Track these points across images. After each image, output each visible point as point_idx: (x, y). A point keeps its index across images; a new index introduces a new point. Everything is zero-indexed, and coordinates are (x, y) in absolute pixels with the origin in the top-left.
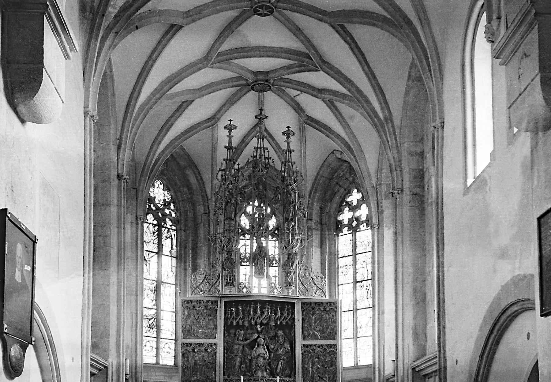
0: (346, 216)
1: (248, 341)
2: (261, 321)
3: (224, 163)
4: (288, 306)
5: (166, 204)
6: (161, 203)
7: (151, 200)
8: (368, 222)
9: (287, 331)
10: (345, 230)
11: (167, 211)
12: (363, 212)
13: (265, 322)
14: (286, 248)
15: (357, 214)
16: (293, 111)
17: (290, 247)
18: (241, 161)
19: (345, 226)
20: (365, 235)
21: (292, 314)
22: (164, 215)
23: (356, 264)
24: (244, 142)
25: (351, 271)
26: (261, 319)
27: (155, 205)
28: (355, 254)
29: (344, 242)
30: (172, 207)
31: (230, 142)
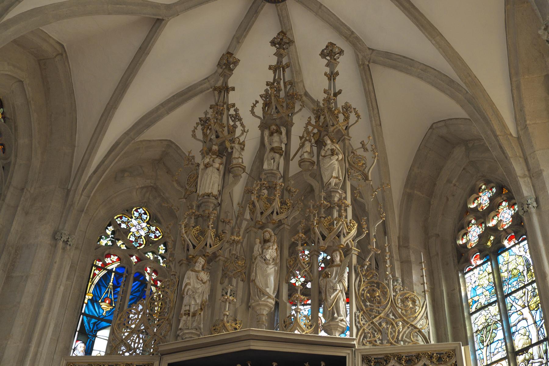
6: (143, 241)
7: (120, 233)
8: (519, 229)
10: (475, 261)
14: (324, 238)
17: (333, 235)
20: (515, 256)
23: (507, 317)
25: (500, 335)
27: (128, 243)
29: (477, 281)
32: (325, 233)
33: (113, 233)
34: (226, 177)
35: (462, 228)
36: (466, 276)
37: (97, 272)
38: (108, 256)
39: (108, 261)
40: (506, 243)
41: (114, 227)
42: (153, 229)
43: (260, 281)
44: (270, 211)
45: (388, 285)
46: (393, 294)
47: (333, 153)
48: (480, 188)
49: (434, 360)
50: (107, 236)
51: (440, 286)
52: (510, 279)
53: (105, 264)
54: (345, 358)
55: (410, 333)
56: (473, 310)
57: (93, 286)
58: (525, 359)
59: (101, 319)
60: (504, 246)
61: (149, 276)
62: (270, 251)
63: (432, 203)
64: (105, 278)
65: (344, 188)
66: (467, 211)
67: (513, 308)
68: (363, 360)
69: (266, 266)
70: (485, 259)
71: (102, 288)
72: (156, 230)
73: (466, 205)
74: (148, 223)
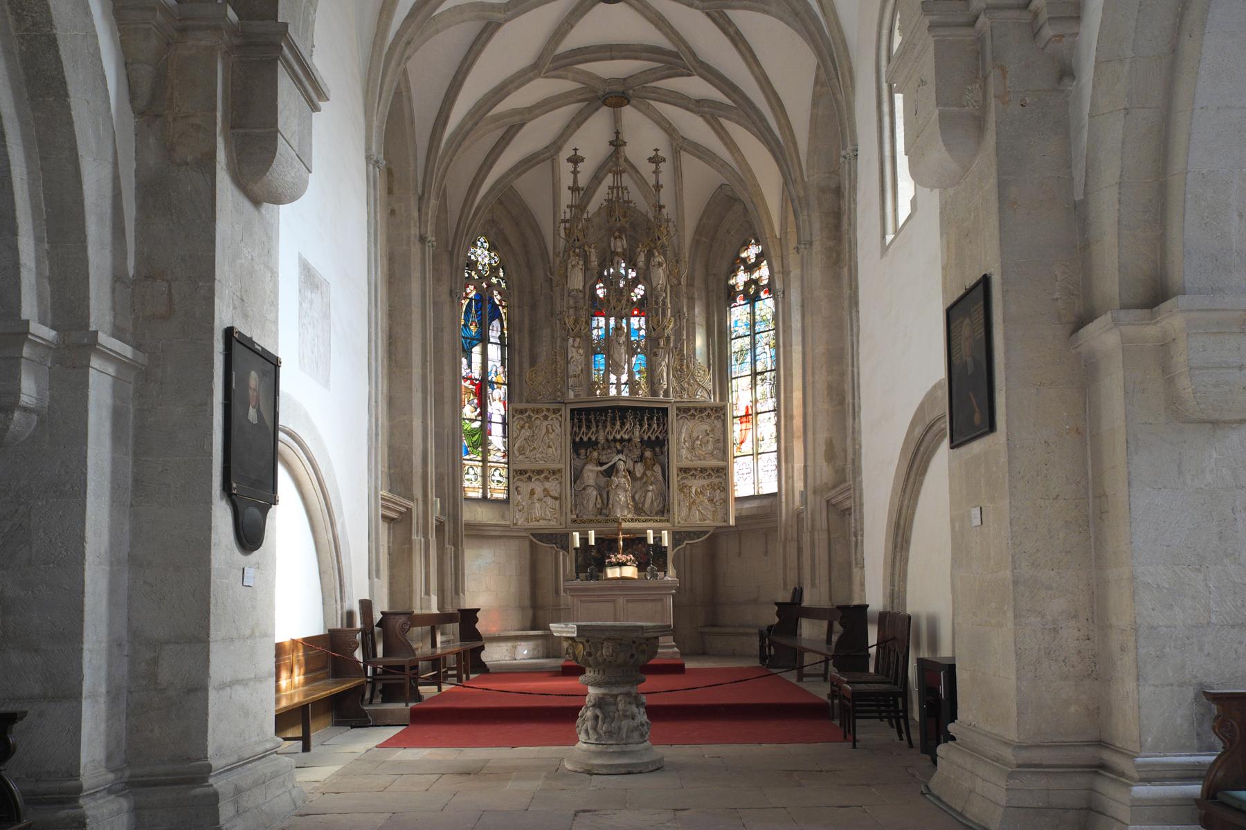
0: (741, 279)
1: (605, 467)
3: (568, 210)
5: (494, 270)
7: (472, 265)
8: (770, 288)
9: (657, 449)
10: (740, 301)
11: (494, 280)
12: (763, 273)
13: (626, 437)
15: (756, 275)
16: (662, 132)
18: (593, 207)
19: (741, 292)
20: (766, 306)
22: (490, 285)
24: (596, 179)
25: (748, 359)
27: (478, 272)
28: (753, 334)
29: (739, 314)
31: (575, 181)
40: (762, 295)
43: (616, 356)
47: (660, 264)
59: (472, 339)
61: (497, 298)
64: (469, 305)
65: (665, 291)
66: (738, 257)
73: (738, 253)
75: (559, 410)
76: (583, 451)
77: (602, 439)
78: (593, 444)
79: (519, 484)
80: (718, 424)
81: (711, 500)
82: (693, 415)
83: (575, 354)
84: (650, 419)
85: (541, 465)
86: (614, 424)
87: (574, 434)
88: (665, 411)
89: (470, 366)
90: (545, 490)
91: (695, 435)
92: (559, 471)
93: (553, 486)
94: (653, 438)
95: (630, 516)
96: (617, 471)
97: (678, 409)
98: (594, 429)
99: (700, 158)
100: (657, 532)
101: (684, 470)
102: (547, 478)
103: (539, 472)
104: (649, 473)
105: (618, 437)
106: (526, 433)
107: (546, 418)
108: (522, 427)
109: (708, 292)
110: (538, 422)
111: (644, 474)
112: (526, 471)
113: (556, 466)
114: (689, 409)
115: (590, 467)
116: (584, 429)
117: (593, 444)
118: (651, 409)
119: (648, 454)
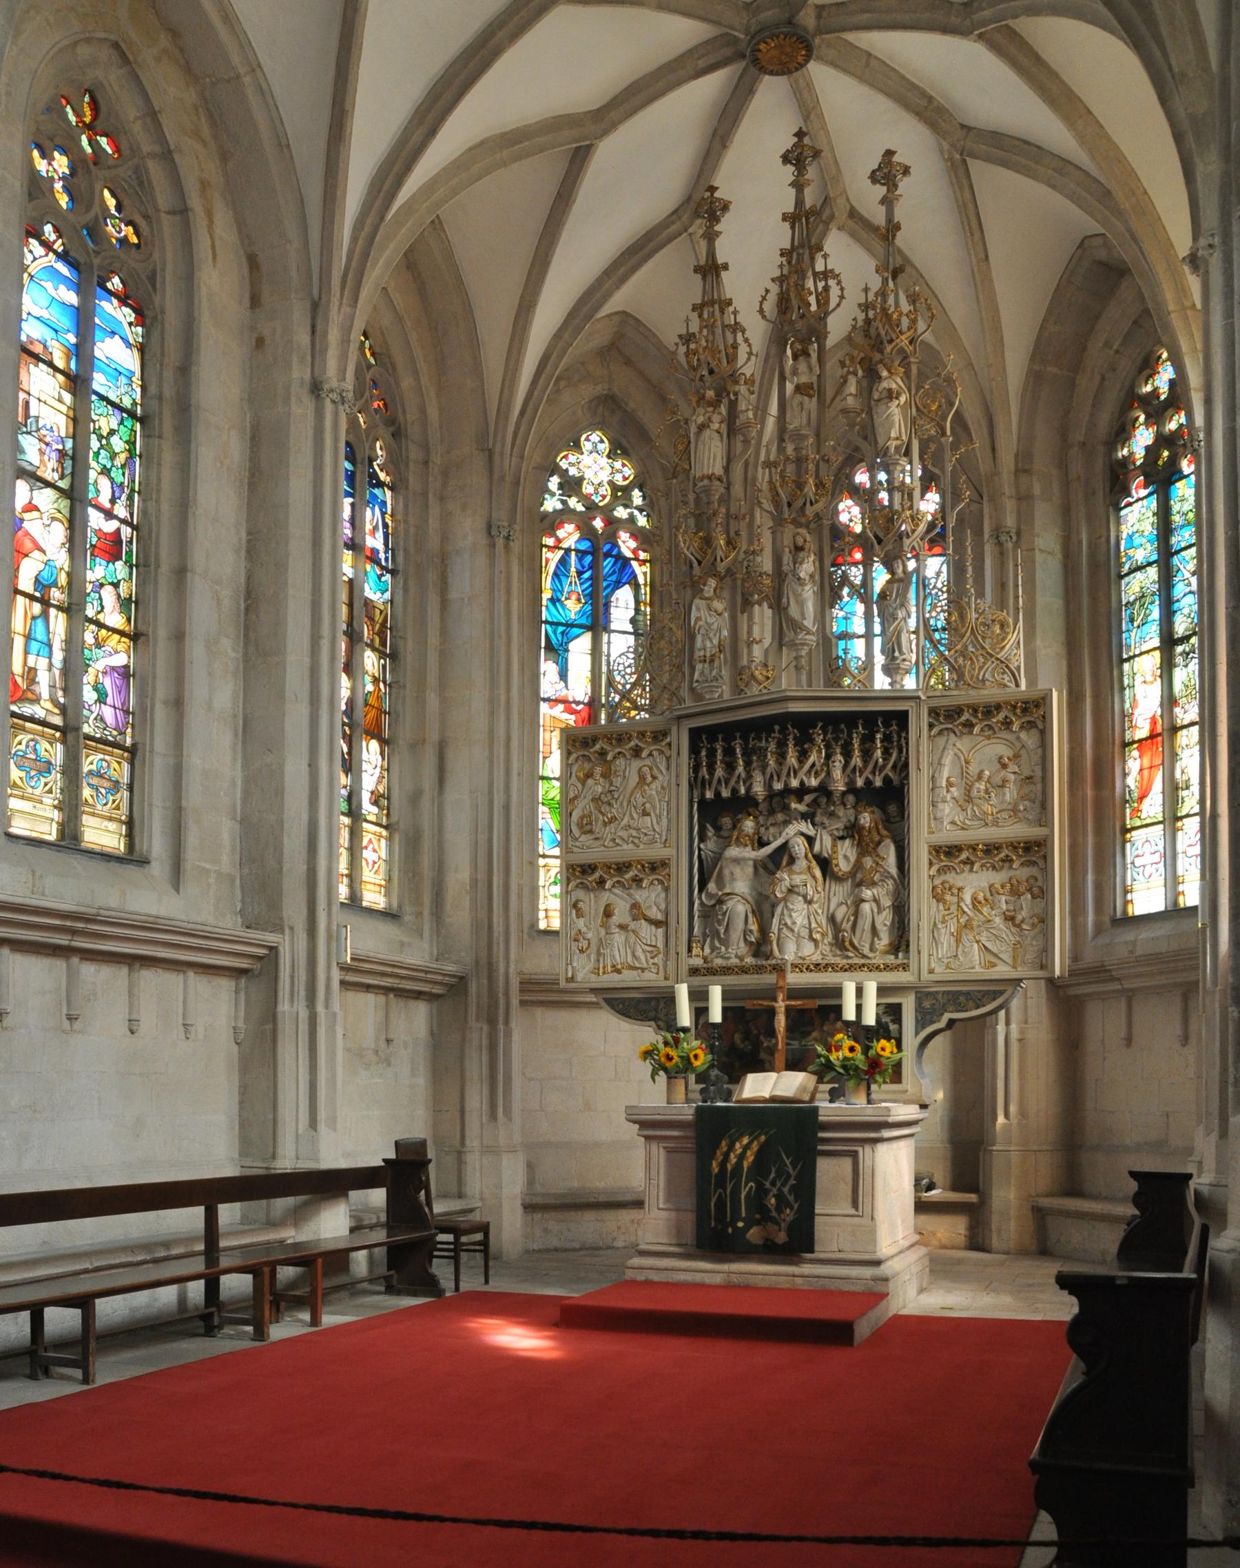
2: (802, 783)
4: (887, 725)
6: (606, 490)
10: (1139, 490)
21: (900, 751)
22: (611, 522)
25: (1155, 613)
26: (801, 775)
30: (637, 497)
32: (881, 535)
33: (561, 486)
34: (732, 442)
35: (1123, 432)
36: (1123, 513)
37: (550, 555)
38: (561, 525)
39: (561, 533)
41: (560, 477)
42: (618, 465)
43: (793, 611)
44: (801, 502)
45: (969, 603)
46: (974, 616)
48: (1160, 357)
49: (1018, 711)
50: (553, 494)
51: (1079, 533)
52: (1183, 526)
53: (559, 541)
54: (906, 712)
55: (994, 669)
56: (1126, 569)
57: (549, 578)
58: (1184, 651)
60: (1180, 471)
62: (805, 566)
63: (1077, 382)
64: (563, 562)
67: (1179, 574)
68: (930, 715)
69: (800, 589)
70: (1150, 489)
71: (563, 579)
72: (624, 465)
74: (609, 457)
75: (665, 734)
76: (726, 821)
77: (759, 789)
78: (743, 804)
79: (580, 894)
80: (1030, 739)
81: (1010, 919)
82: (969, 725)
83: (704, 613)
84: (868, 739)
85: (627, 851)
86: (781, 756)
87: (696, 783)
88: (902, 718)
89: (563, 675)
90: (635, 906)
91: (973, 769)
92: (664, 864)
93: (650, 897)
94: (878, 782)
95: (817, 958)
96: (792, 860)
97: (934, 712)
98: (740, 769)
99: (1005, 164)
100: (860, 992)
101: (947, 853)
102: (637, 881)
103: (622, 868)
104: (868, 862)
105: (795, 783)
106: (597, 786)
107: (637, 752)
108: (589, 775)
109: (1066, 485)
110: (620, 762)
111: (858, 866)
112: (592, 868)
113: (657, 852)
114: (959, 711)
115: (733, 851)
116: (720, 772)
117: (743, 804)
118: (870, 719)
119: (866, 819)
